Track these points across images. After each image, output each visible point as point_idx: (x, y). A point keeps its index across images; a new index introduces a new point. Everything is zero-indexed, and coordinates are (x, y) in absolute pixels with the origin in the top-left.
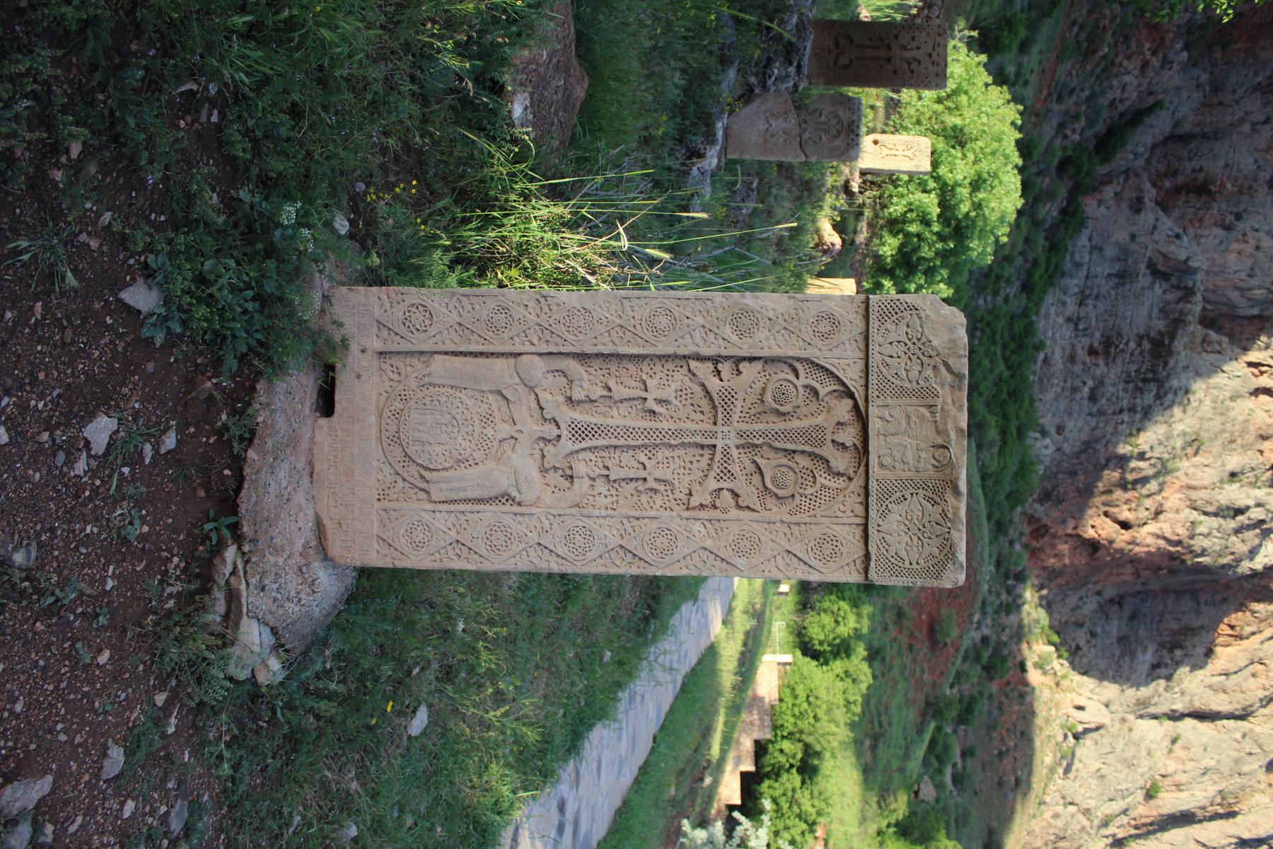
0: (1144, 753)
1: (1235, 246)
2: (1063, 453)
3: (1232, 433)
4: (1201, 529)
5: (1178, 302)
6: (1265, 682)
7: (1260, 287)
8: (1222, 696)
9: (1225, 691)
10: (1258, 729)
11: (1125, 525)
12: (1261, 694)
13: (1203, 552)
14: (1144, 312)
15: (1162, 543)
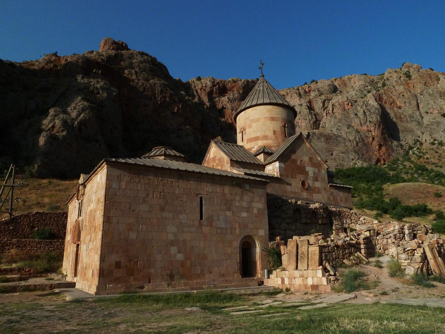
0: (434, 120)
1: (300, 124)
2: (359, 158)
3: (345, 117)
4: (371, 119)
5: (316, 136)
6: (405, 93)
7: (309, 117)
8: (412, 102)
9: (410, 102)
10: (419, 92)
11: (373, 139)
12: (409, 93)
13: (377, 118)
14: (320, 143)
15: (376, 129)
